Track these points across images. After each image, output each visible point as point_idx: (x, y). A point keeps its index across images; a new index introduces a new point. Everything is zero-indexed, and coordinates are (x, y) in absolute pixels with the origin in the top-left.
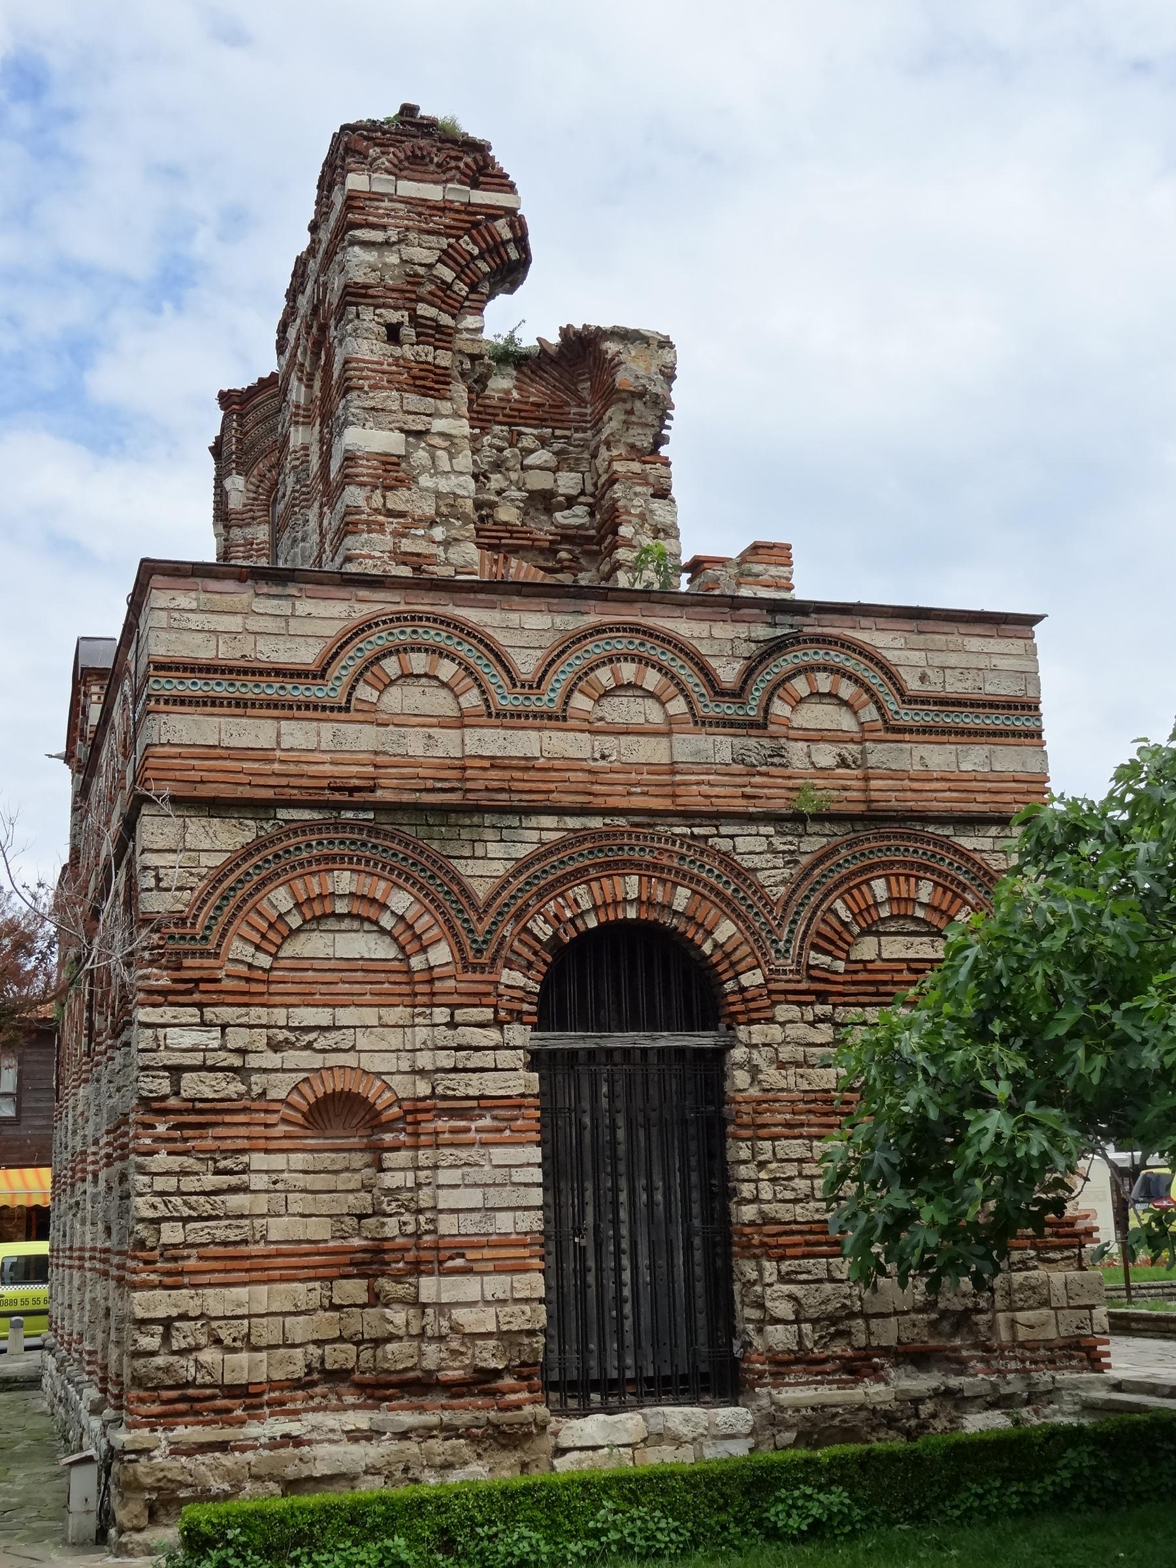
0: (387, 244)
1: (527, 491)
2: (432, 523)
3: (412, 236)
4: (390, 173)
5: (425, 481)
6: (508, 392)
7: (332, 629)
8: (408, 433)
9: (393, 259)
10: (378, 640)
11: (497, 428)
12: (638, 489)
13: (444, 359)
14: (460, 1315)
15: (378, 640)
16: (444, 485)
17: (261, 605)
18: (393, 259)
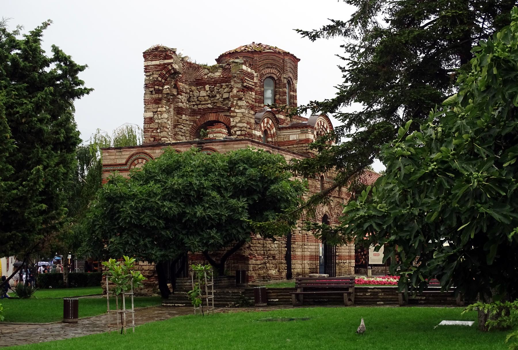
0: (150, 75)
1: (224, 99)
2: (158, 129)
3: (154, 72)
4: (150, 61)
5: (156, 121)
6: (220, 76)
7: (127, 157)
8: (153, 112)
9: (151, 78)
10: (134, 157)
11: (217, 85)
12: (235, 99)
13: (160, 96)
14: (144, 267)
15: (134, 157)
16: (160, 121)
17: (117, 154)
18: (151, 78)
